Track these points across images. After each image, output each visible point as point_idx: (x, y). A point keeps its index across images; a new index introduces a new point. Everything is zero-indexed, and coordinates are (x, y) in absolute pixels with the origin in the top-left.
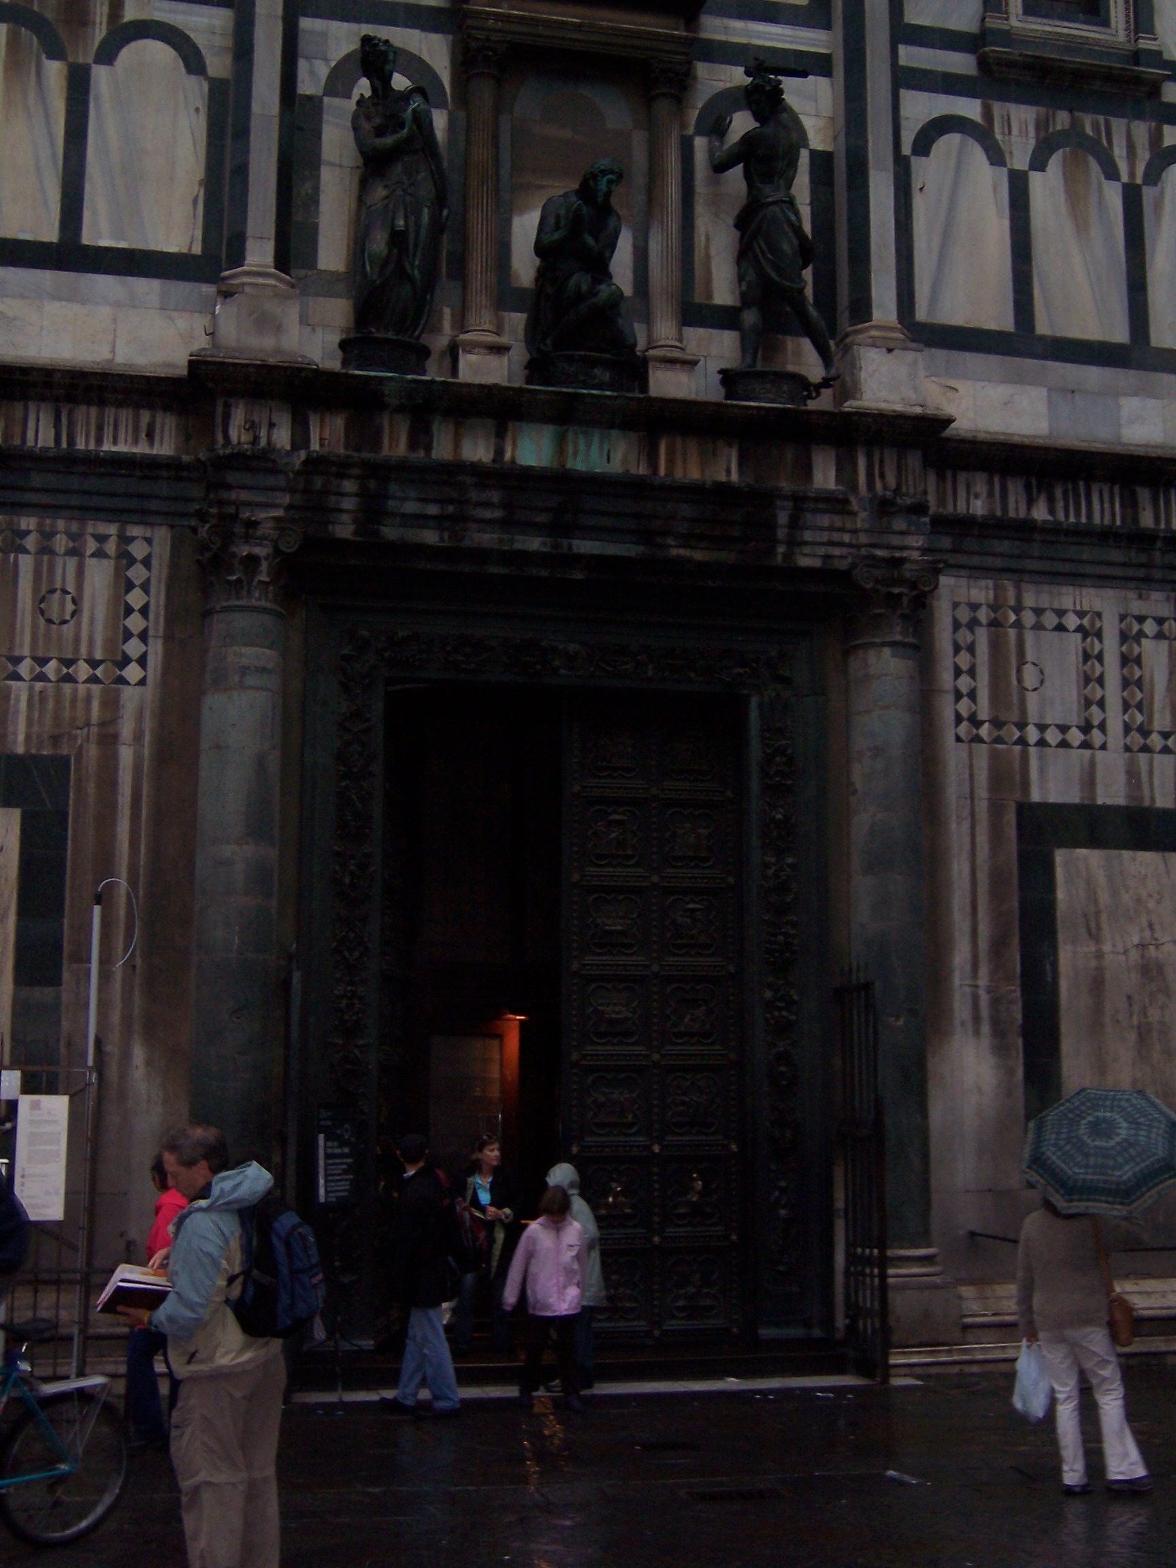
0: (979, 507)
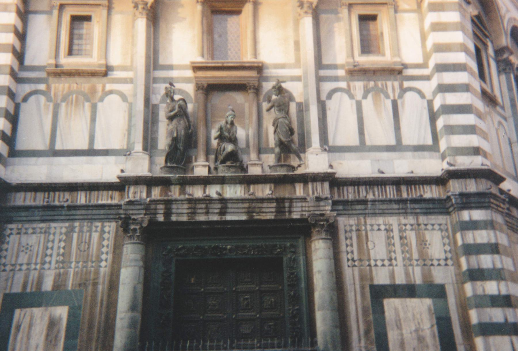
0: (351, 197)
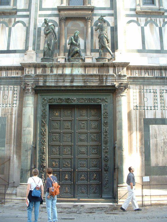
0: (137, 75)
